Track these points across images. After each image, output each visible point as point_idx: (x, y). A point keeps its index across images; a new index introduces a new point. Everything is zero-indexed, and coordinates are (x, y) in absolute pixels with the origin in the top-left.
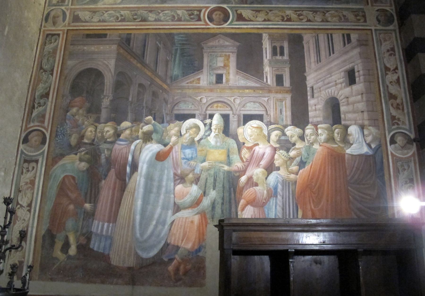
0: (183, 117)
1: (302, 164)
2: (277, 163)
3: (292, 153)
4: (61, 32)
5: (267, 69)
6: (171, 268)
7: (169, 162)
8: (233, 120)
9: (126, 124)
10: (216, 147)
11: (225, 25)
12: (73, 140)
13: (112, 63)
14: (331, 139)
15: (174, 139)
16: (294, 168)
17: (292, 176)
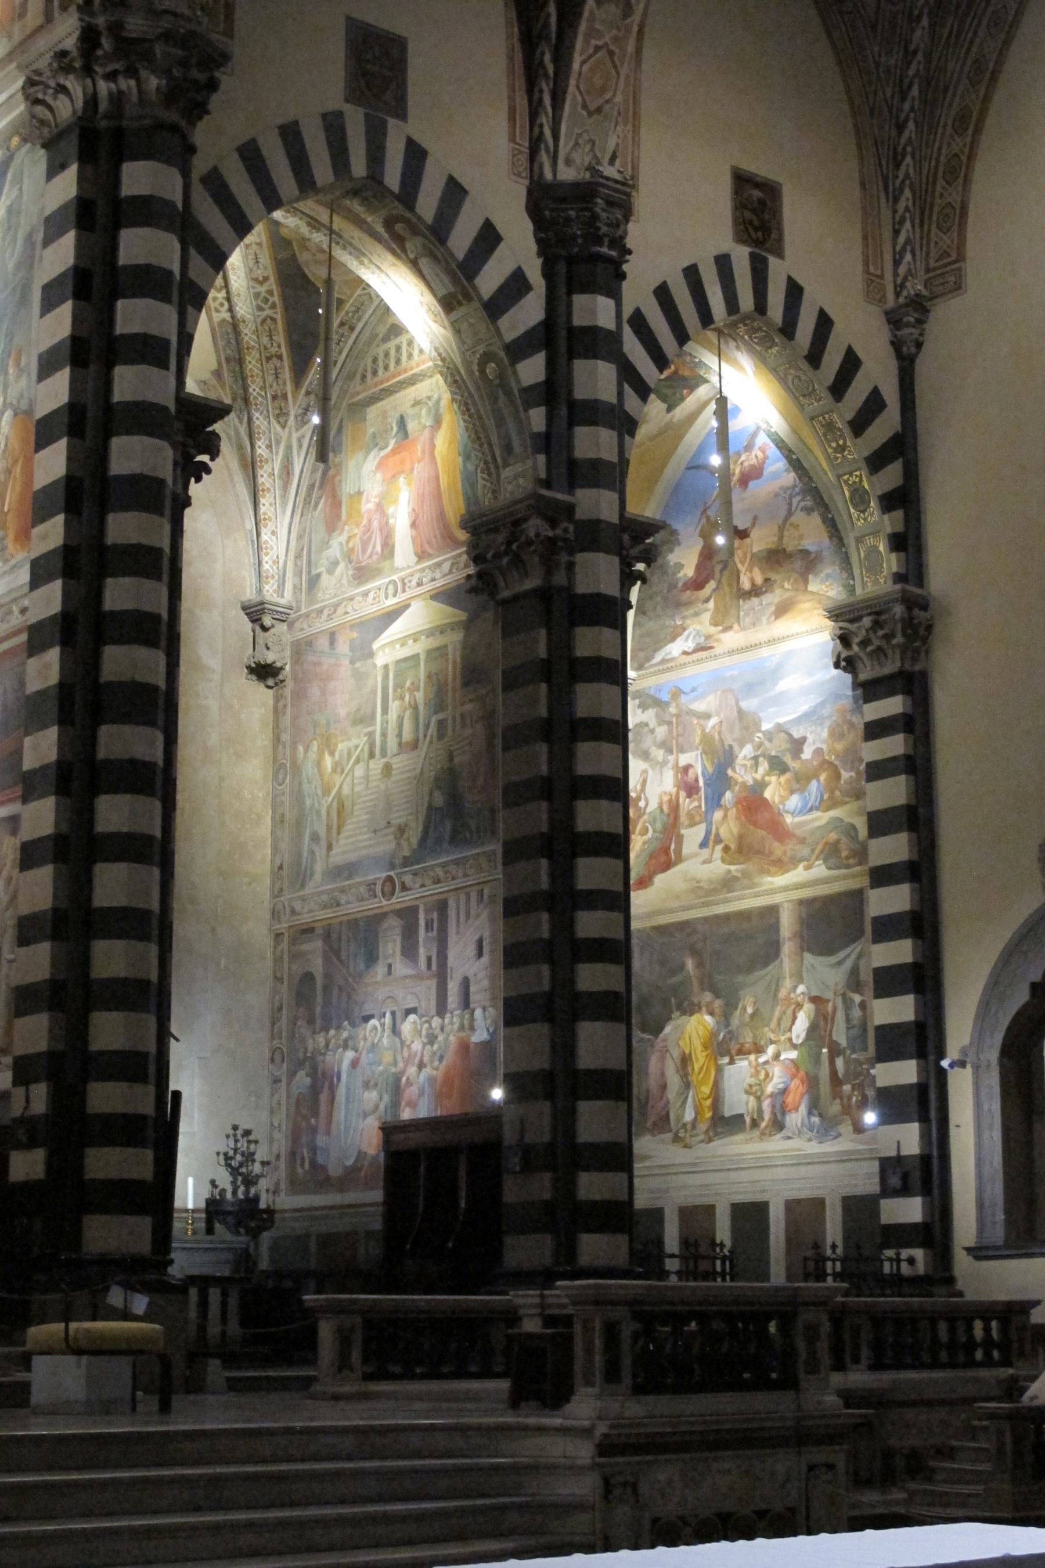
0: (367, 1019)
1: (441, 1058)
2: (426, 1059)
3: (435, 1047)
4: (284, 931)
5: (422, 951)
6: (363, 1174)
7: (359, 1070)
8: (398, 1015)
9: (332, 1032)
10: (387, 1049)
11: (394, 900)
12: (301, 1055)
13: (319, 961)
14: (462, 1027)
15: (362, 1043)
16: (436, 1063)
17: (435, 1072)
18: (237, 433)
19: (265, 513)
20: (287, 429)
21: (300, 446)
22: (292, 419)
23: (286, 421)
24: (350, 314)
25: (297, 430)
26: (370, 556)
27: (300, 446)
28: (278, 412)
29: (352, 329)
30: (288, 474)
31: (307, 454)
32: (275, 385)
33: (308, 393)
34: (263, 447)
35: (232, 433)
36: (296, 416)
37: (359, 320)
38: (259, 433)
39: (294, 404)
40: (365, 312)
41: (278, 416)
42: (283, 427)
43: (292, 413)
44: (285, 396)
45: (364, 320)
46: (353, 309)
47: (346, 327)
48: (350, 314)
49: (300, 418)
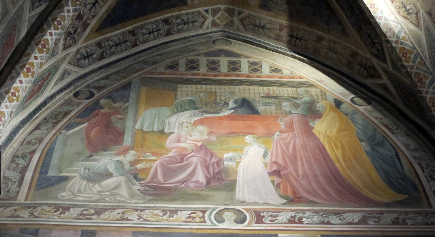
18: (19, 16)
19: (17, 89)
20: (65, 53)
21: (62, 78)
22: (73, 49)
23: (70, 46)
24: (179, 21)
25: (70, 63)
26: (183, 181)
27: (62, 78)
28: (72, 30)
29: (168, 33)
30: (40, 88)
31: (64, 88)
32: (89, 7)
33: (99, 44)
34: (54, 37)
35: (13, 11)
36: (78, 51)
37: (179, 31)
38: (59, 23)
39: (85, 41)
40: (189, 30)
41: (69, 34)
42: (65, 48)
43: (79, 45)
44: (86, 26)
45: (182, 35)
46: (185, 18)
47: (166, 27)
48: (179, 21)
49: (78, 56)
